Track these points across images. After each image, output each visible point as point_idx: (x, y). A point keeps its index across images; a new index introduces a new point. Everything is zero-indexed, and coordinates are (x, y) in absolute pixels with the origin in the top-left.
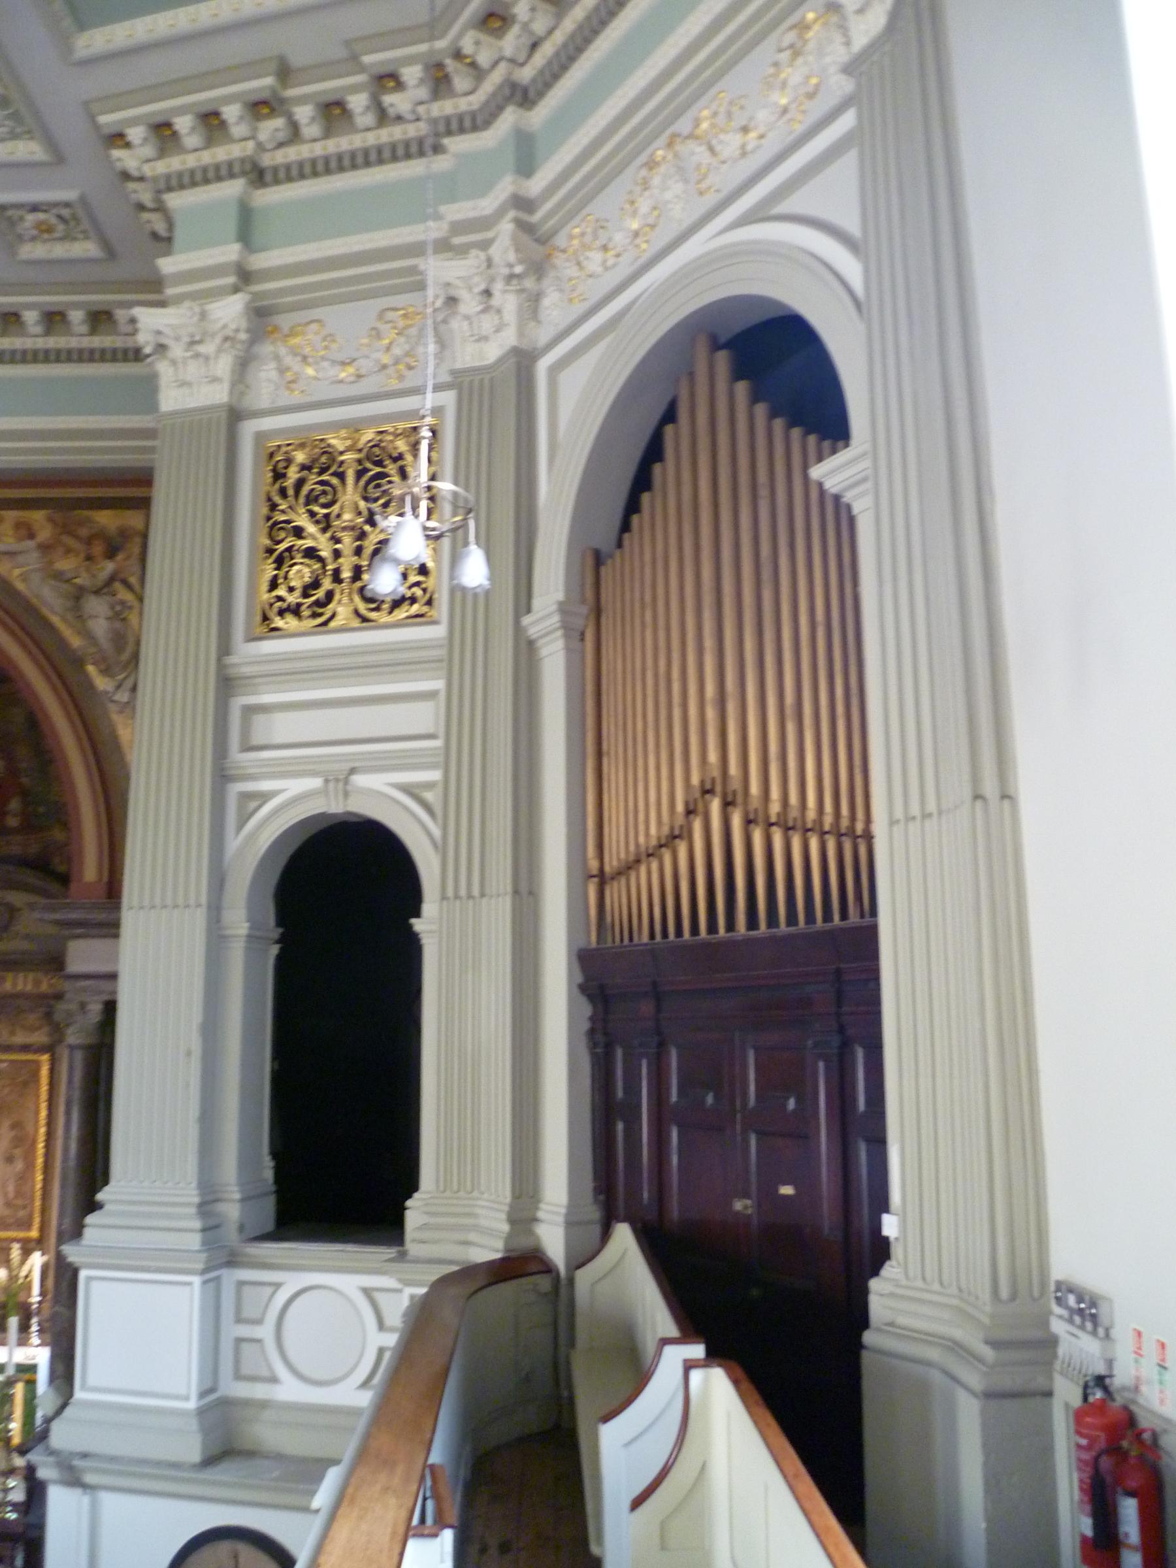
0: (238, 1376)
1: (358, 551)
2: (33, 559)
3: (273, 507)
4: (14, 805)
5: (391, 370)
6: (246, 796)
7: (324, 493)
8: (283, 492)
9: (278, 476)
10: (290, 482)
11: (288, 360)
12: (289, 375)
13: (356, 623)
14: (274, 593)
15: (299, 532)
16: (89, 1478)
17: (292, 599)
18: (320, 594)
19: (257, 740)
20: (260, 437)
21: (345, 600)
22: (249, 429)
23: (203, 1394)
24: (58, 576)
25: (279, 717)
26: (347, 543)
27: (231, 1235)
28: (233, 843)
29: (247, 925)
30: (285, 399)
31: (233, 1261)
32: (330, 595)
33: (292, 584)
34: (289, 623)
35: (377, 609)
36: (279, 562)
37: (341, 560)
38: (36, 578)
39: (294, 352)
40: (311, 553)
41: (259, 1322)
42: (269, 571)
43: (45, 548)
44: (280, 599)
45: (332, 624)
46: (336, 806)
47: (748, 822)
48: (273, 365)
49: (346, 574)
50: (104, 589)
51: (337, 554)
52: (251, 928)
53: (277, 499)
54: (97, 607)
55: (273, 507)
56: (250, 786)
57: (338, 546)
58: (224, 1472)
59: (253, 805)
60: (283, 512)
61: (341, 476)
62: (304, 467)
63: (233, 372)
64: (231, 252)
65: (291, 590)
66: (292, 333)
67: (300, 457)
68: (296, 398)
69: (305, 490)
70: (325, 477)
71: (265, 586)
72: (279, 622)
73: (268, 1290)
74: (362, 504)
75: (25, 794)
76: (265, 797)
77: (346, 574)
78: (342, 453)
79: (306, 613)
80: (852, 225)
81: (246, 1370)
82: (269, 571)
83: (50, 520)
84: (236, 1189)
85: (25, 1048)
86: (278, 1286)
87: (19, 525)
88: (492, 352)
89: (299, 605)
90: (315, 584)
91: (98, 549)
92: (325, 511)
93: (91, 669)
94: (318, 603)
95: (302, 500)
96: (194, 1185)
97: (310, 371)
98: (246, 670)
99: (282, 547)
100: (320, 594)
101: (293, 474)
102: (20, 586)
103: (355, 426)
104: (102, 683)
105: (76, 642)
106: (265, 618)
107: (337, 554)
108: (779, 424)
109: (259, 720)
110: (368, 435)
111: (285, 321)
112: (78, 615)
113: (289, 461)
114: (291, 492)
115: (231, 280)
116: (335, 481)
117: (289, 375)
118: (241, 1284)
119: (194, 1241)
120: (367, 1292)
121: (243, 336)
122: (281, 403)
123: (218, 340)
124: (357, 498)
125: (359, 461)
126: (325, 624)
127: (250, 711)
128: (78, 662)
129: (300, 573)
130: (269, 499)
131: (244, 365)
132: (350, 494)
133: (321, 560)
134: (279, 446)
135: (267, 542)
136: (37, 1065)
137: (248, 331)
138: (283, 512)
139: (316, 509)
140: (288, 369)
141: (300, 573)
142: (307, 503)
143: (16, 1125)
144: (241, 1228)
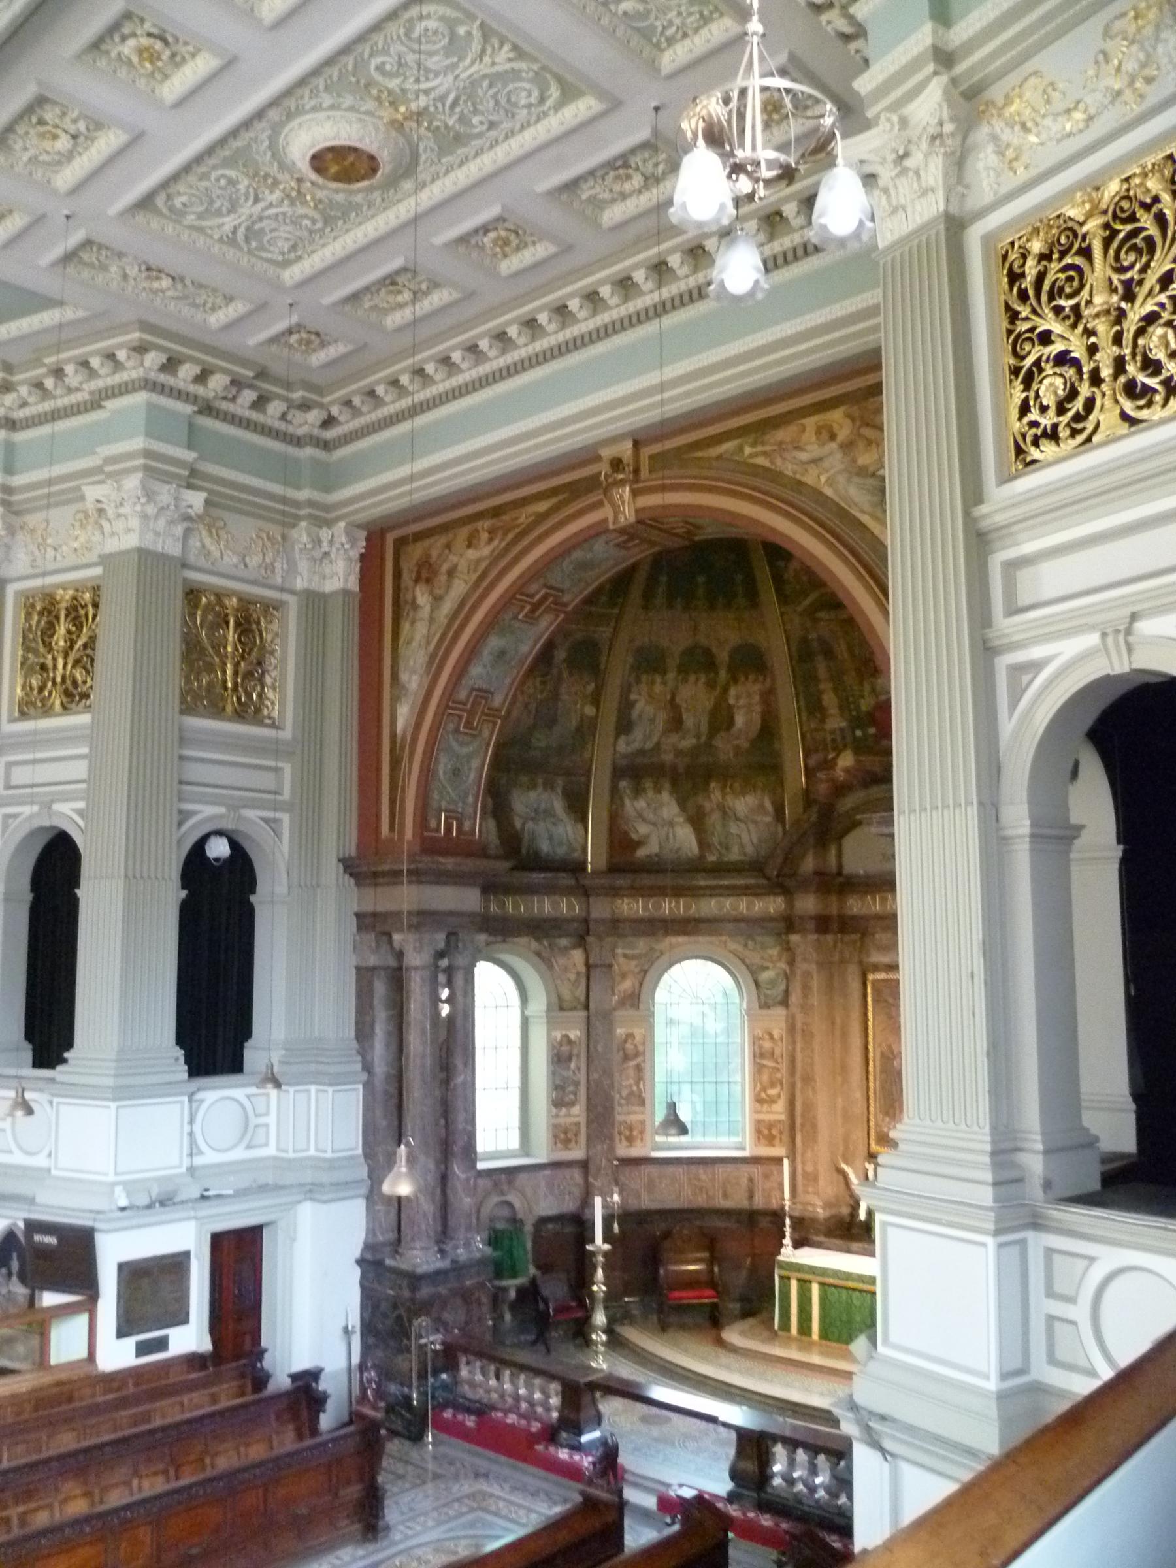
0: (1052, 1360)
1: (1118, 340)
2: (836, 460)
3: (1014, 317)
5: (1128, 95)
6: (1018, 670)
7: (1070, 279)
8: (1023, 296)
9: (1014, 277)
10: (1028, 283)
11: (1006, 135)
12: (1010, 154)
13: (1124, 428)
14: (1025, 420)
15: (1046, 338)
16: (888, 1444)
17: (1046, 421)
18: (1078, 405)
19: (1024, 599)
20: (988, 240)
21: (1108, 402)
22: (974, 237)
23: (1004, 1376)
25: (1047, 568)
26: (1103, 328)
27: (1035, 1191)
28: (1007, 726)
29: (1028, 822)
30: (1011, 182)
31: (1037, 1223)
32: (1090, 404)
33: (1045, 403)
34: (1048, 449)
35: (1150, 404)
36: (1028, 383)
37: (1098, 356)
38: (841, 479)
39: (1010, 124)
41: (1071, 1300)
42: (1018, 394)
43: (847, 446)
44: (1034, 424)
45: (1095, 439)
46: (1120, 666)
48: (990, 148)
49: (1106, 372)
51: (1093, 350)
52: (1032, 825)
53: (1018, 307)
55: (1014, 317)
56: (1019, 657)
57: (1093, 339)
59: (1025, 679)
60: (1027, 319)
61: (1086, 253)
62: (1045, 257)
63: (946, 175)
64: (924, 36)
65: (1044, 409)
66: (1008, 101)
67: (1037, 246)
68: (1023, 175)
69: (1046, 286)
70: (1068, 260)
71: (1014, 413)
72: (1035, 453)
73: (1081, 1264)
74: (1115, 278)
76: (1035, 667)
77: (1106, 372)
78: (1081, 224)
79: (1064, 433)
81: (1060, 1355)
82: (1018, 394)
83: (849, 416)
84: (1039, 1138)
86: (1092, 1259)
89: (1055, 426)
90: (1073, 394)
92: (1072, 302)
94: (1078, 418)
95: (1044, 297)
96: (987, 1129)
97: (1033, 139)
98: (999, 519)
99: (1028, 362)
100: (1078, 405)
101: (1031, 269)
102: (828, 492)
106: (1019, 451)
107: (1093, 350)
109: (1024, 576)
110: (1114, 187)
111: (996, 93)
114: (1031, 293)
115: (931, 67)
116: (1078, 261)
117: (1010, 154)
118: (1050, 1252)
119: (986, 1195)
121: (949, 128)
122: (1004, 190)
123: (924, 145)
124: (1109, 272)
125: (1107, 226)
126: (1089, 440)
127: (1013, 565)
129: (1051, 386)
130: (1008, 307)
131: (959, 163)
132: (1100, 270)
133: (1076, 363)
134: (1012, 244)
135: (1012, 361)
137: (953, 119)
138: (1027, 319)
139: (1062, 302)
140: (1008, 146)
141: (1051, 386)
142: (1051, 298)
144: (1047, 1185)
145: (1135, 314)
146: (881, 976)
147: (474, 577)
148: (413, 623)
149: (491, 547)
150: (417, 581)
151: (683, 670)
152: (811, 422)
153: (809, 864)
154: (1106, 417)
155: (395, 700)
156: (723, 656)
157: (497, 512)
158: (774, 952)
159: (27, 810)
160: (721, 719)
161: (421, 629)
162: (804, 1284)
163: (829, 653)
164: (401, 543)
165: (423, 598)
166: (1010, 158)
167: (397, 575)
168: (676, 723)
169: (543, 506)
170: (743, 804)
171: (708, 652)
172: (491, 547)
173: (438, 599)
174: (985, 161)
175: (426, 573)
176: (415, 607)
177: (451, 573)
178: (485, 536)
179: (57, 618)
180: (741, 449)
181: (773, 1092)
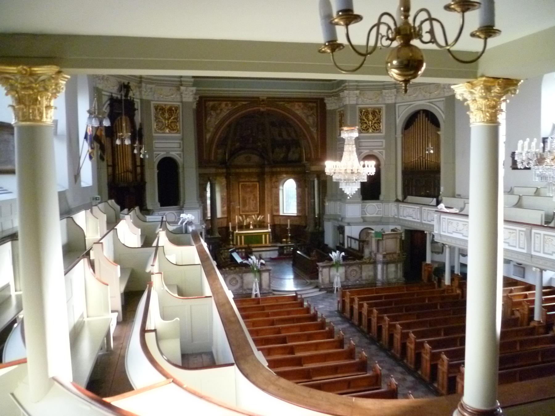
1: (372, 123)
3: (360, 116)
4: (251, 139)
8: (362, 115)
9: (361, 112)
15: (364, 120)
18: (367, 128)
20: (359, 107)
24: (304, 113)
40: (366, 123)
43: (302, 109)
47: (425, 160)
49: (370, 126)
50: (311, 116)
56: (360, 151)
58: (365, 222)
61: (369, 113)
62: (364, 112)
67: (364, 111)
77: (370, 126)
80: (443, 110)
85: (254, 182)
86: (366, 205)
87: (298, 105)
88: (390, 102)
90: (366, 127)
91: (310, 109)
93: (310, 127)
100: (367, 128)
103: (371, 108)
104: (312, 130)
105: (308, 123)
108: (431, 124)
113: (362, 111)
120: (376, 205)
132: (371, 117)
136: (257, 184)
141: (365, 126)
143: (254, 195)
146: (243, 183)
147: (228, 112)
148: (211, 118)
149: (232, 107)
150: (212, 109)
152: (297, 103)
154: (370, 130)
158: (224, 180)
159: (162, 153)
161: (213, 120)
162: (241, 237)
164: (206, 101)
166: (363, 101)
169: (244, 103)
172: (232, 107)
173: (218, 115)
174: (360, 99)
175: (214, 108)
176: (211, 114)
177: (221, 110)
178: (230, 105)
179: (165, 111)
180: (284, 104)
181: (224, 205)
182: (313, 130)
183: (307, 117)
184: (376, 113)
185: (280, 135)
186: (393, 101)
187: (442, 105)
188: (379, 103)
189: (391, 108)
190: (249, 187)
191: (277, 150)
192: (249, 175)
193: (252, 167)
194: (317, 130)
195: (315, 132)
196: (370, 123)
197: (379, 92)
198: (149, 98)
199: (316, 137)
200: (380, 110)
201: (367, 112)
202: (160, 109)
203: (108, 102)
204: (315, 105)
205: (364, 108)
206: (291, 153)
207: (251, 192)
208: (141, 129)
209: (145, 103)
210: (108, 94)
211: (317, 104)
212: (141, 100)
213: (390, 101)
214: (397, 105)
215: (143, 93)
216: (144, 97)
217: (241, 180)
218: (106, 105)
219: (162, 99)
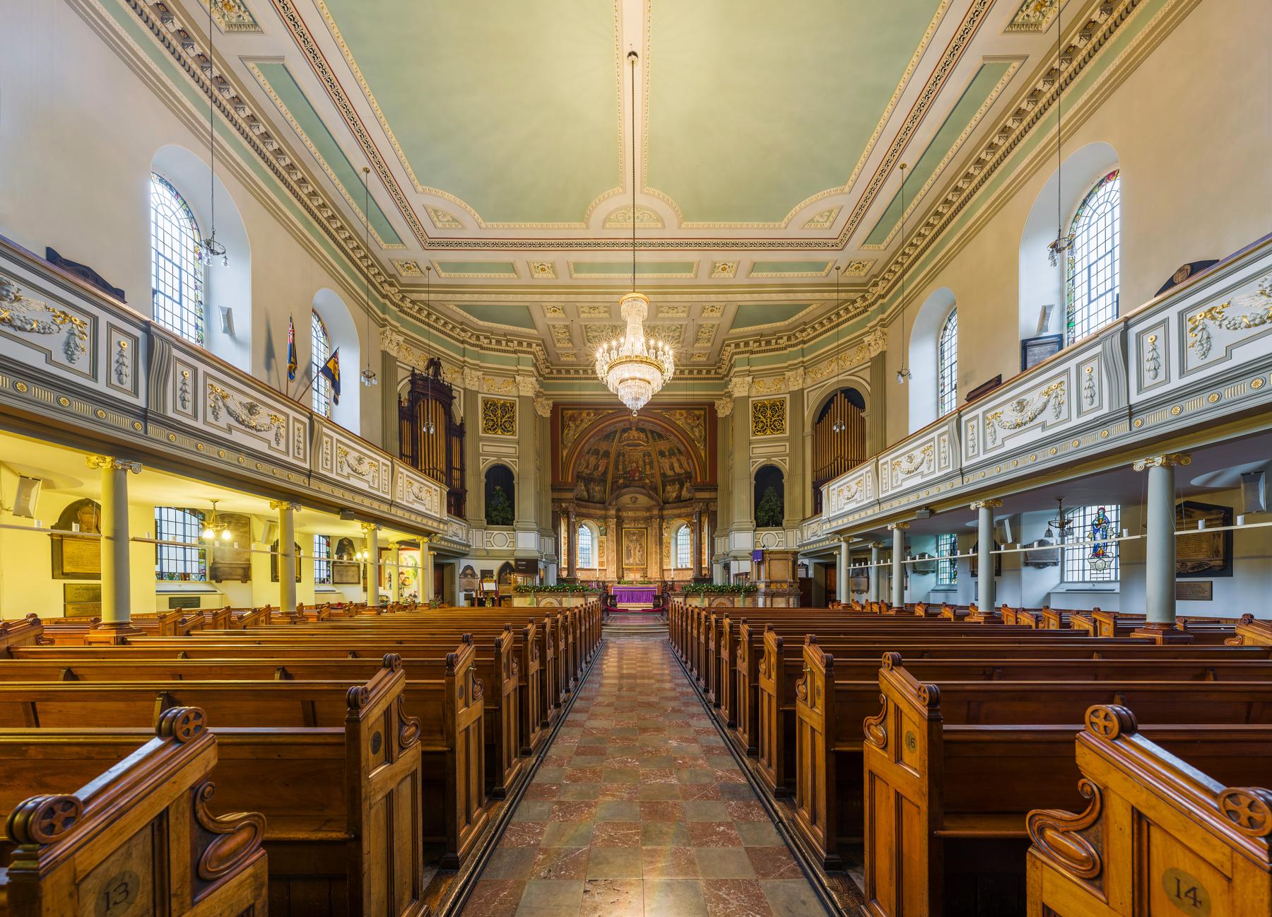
4: (637, 474)
40: (762, 422)
54: (696, 430)
75: (640, 472)
88: (796, 388)
103: (770, 400)
112: (694, 433)
128: (693, 441)
132: (769, 412)
141: (761, 425)
145: (773, 419)
151: (593, 454)
152: (678, 411)
153: (614, 503)
155: (563, 449)
156: (601, 452)
157: (596, 409)
160: (596, 467)
161: (572, 433)
163: (624, 456)
164: (563, 409)
165: (572, 425)
167: (563, 417)
168: (587, 467)
169: (610, 412)
170: (597, 489)
171: (599, 451)
173: (577, 426)
175: (573, 418)
176: (569, 426)
177: (582, 421)
178: (592, 414)
182: (700, 446)
183: (693, 427)
184: (776, 407)
185: (672, 468)
186: (801, 387)
187: (867, 375)
188: (780, 392)
189: (798, 396)
190: (634, 534)
191: (669, 488)
192: (635, 520)
193: (638, 510)
194: (705, 446)
195: (702, 447)
196: (769, 420)
197: (781, 377)
198: (475, 388)
199: (703, 455)
200: (782, 403)
201: (764, 406)
202: (490, 406)
203: (410, 378)
204: (703, 412)
205: (760, 401)
206: (685, 489)
207: (637, 540)
208: (462, 424)
209: (470, 395)
210: (411, 369)
211: (705, 412)
212: (465, 389)
213: (795, 386)
214: (805, 392)
215: (467, 381)
216: (468, 387)
217: (625, 526)
218: (406, 381)
219: (493, 392)
